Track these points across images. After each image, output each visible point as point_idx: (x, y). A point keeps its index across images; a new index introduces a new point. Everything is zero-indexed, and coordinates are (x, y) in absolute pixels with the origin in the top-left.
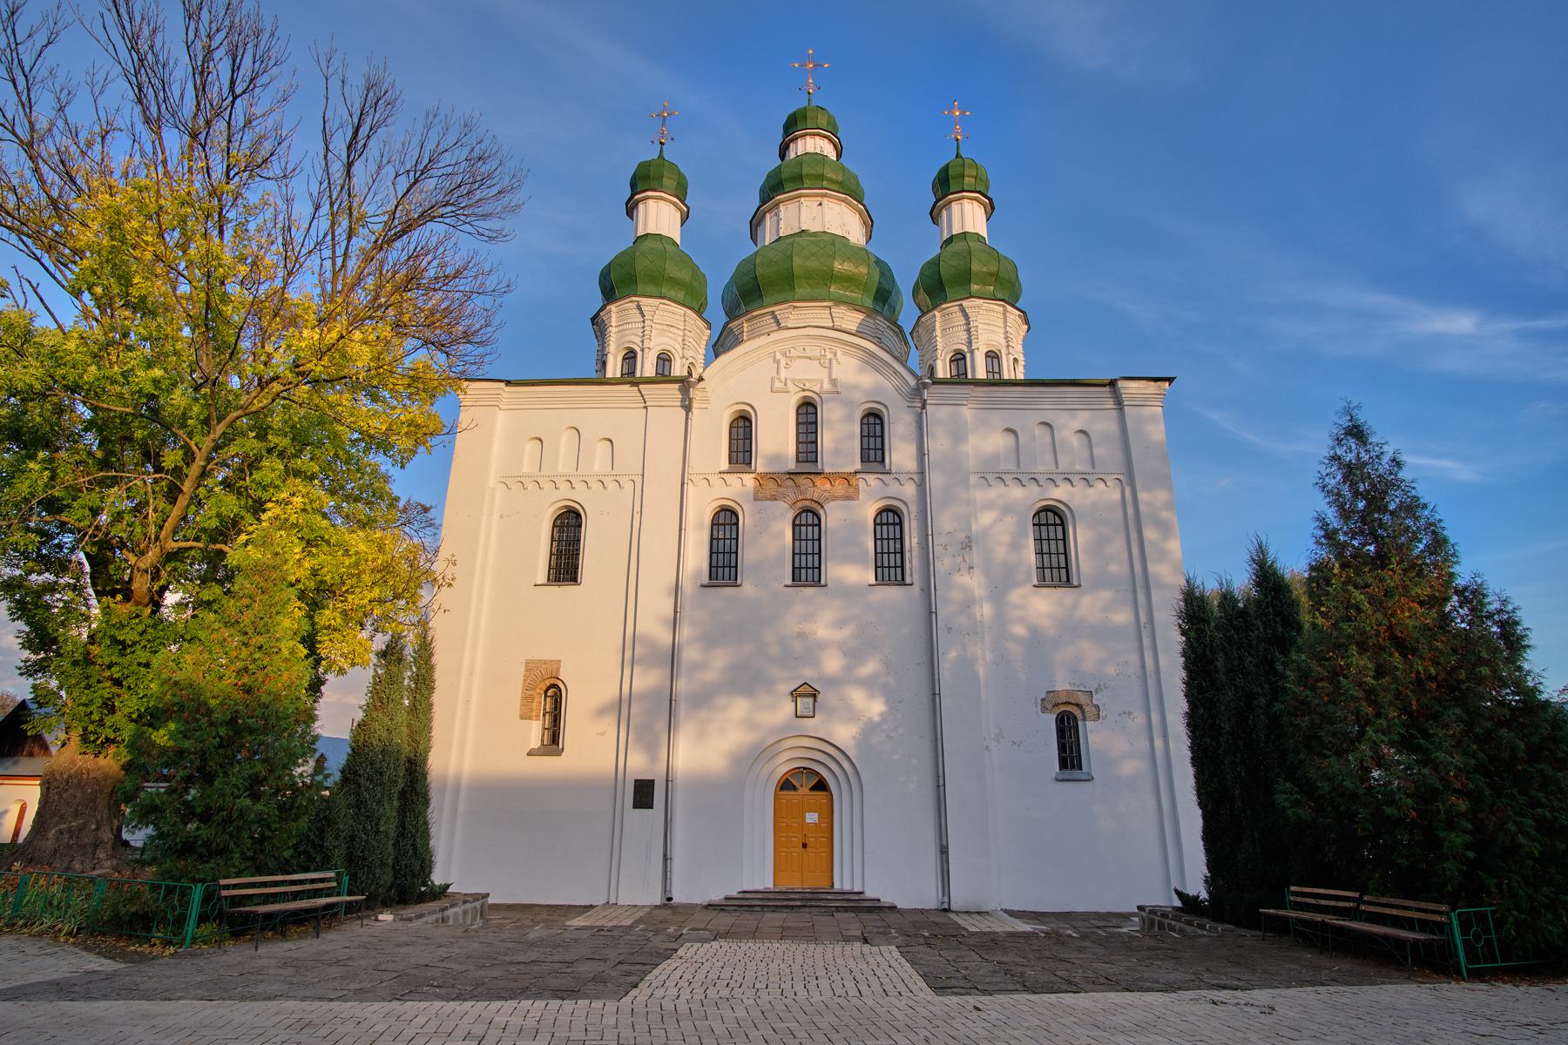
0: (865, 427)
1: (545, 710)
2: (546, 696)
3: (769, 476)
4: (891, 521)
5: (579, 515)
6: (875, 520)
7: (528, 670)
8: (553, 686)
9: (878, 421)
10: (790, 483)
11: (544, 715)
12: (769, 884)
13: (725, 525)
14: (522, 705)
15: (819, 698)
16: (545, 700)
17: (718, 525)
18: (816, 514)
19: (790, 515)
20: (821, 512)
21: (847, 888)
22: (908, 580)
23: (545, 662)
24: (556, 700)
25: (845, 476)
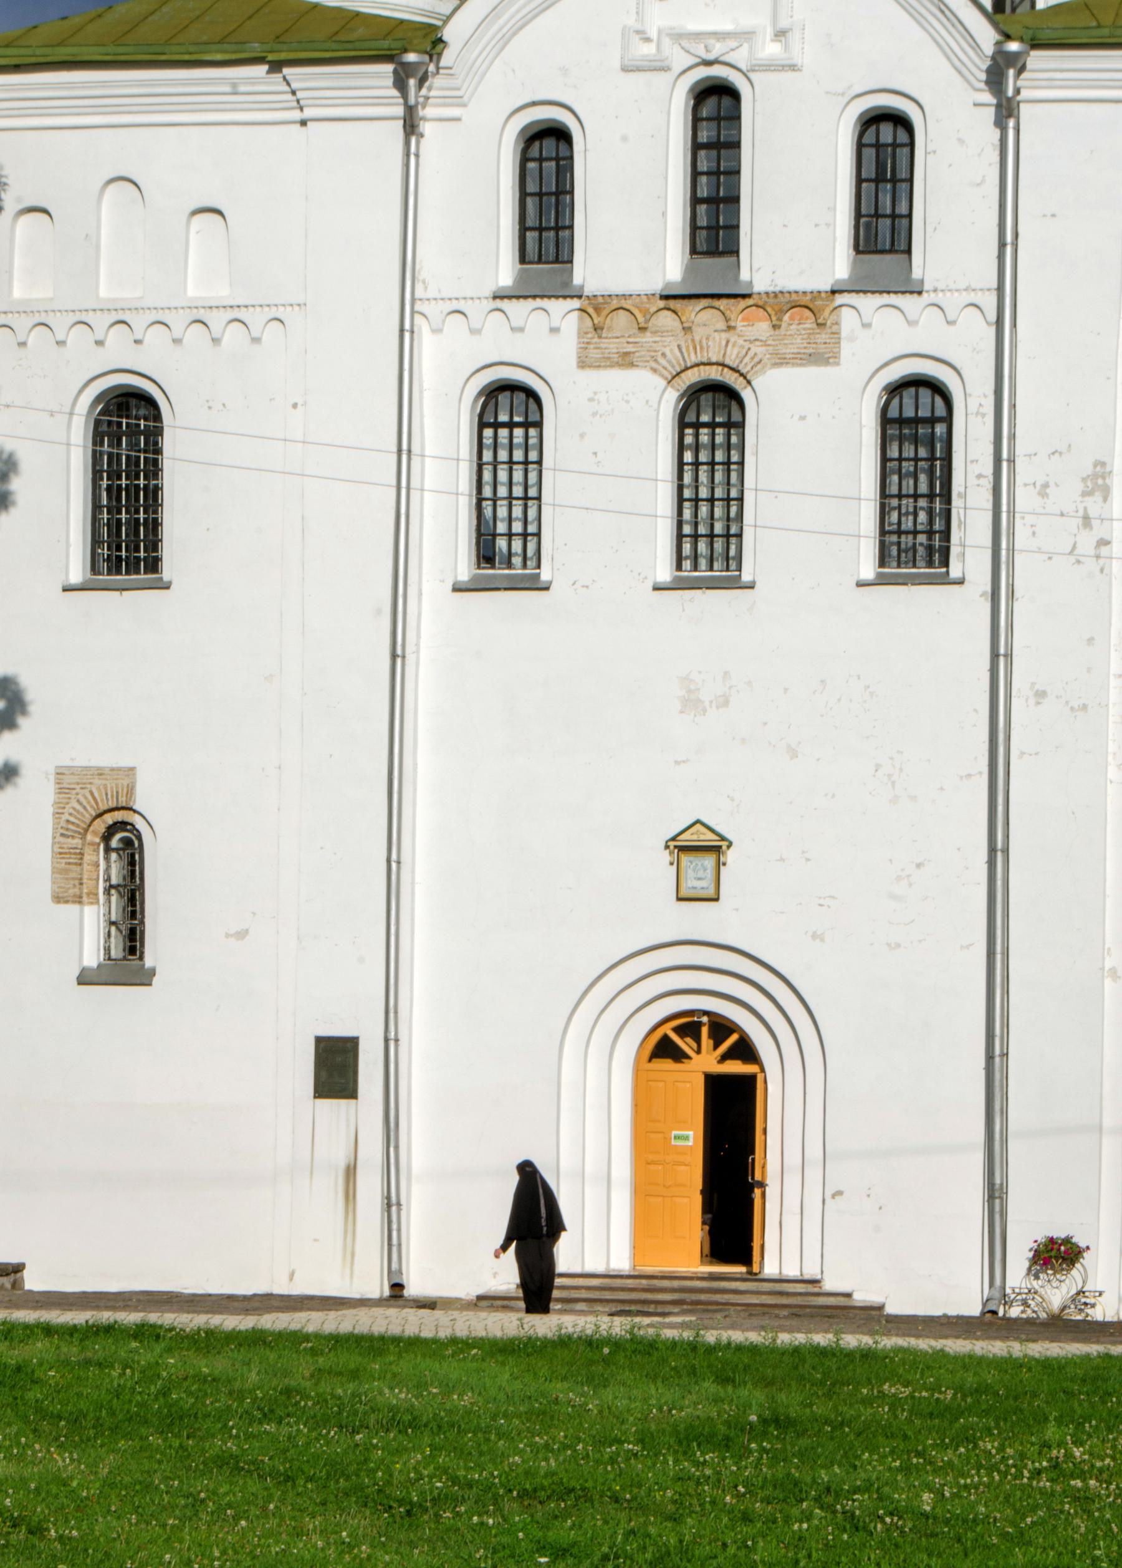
0: (869, 154)
1: (108, 879)
2: (108, 850)
3: (615, 303)
4: (924, 413)
5: (149, 402)
6: (884, 410)
7: (63, 790)
8: (122, 825)
9: (902, 136)
10: (666, 320)
11: (107, 892)
12: (621, 1261)
13: (511, 425)
14: (55, 871)
15: (731, 856)
16: (107, 859)
17: (496, 425)
18: (733, 396)
19: (669, 402)
20: (746, 395)
21: (791, 1271)
22: (955, 571)
23: (100, 772)
24: (132, 863)
25: (806, 300)
